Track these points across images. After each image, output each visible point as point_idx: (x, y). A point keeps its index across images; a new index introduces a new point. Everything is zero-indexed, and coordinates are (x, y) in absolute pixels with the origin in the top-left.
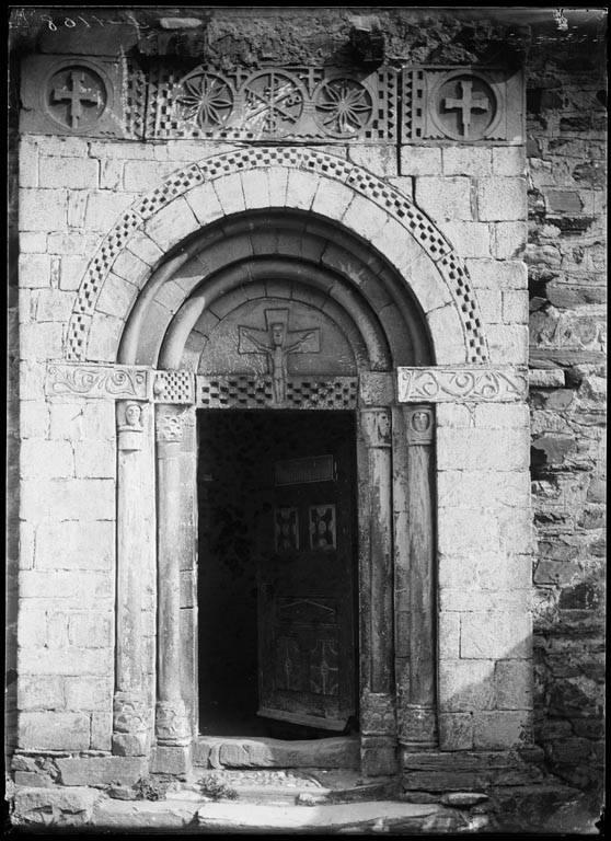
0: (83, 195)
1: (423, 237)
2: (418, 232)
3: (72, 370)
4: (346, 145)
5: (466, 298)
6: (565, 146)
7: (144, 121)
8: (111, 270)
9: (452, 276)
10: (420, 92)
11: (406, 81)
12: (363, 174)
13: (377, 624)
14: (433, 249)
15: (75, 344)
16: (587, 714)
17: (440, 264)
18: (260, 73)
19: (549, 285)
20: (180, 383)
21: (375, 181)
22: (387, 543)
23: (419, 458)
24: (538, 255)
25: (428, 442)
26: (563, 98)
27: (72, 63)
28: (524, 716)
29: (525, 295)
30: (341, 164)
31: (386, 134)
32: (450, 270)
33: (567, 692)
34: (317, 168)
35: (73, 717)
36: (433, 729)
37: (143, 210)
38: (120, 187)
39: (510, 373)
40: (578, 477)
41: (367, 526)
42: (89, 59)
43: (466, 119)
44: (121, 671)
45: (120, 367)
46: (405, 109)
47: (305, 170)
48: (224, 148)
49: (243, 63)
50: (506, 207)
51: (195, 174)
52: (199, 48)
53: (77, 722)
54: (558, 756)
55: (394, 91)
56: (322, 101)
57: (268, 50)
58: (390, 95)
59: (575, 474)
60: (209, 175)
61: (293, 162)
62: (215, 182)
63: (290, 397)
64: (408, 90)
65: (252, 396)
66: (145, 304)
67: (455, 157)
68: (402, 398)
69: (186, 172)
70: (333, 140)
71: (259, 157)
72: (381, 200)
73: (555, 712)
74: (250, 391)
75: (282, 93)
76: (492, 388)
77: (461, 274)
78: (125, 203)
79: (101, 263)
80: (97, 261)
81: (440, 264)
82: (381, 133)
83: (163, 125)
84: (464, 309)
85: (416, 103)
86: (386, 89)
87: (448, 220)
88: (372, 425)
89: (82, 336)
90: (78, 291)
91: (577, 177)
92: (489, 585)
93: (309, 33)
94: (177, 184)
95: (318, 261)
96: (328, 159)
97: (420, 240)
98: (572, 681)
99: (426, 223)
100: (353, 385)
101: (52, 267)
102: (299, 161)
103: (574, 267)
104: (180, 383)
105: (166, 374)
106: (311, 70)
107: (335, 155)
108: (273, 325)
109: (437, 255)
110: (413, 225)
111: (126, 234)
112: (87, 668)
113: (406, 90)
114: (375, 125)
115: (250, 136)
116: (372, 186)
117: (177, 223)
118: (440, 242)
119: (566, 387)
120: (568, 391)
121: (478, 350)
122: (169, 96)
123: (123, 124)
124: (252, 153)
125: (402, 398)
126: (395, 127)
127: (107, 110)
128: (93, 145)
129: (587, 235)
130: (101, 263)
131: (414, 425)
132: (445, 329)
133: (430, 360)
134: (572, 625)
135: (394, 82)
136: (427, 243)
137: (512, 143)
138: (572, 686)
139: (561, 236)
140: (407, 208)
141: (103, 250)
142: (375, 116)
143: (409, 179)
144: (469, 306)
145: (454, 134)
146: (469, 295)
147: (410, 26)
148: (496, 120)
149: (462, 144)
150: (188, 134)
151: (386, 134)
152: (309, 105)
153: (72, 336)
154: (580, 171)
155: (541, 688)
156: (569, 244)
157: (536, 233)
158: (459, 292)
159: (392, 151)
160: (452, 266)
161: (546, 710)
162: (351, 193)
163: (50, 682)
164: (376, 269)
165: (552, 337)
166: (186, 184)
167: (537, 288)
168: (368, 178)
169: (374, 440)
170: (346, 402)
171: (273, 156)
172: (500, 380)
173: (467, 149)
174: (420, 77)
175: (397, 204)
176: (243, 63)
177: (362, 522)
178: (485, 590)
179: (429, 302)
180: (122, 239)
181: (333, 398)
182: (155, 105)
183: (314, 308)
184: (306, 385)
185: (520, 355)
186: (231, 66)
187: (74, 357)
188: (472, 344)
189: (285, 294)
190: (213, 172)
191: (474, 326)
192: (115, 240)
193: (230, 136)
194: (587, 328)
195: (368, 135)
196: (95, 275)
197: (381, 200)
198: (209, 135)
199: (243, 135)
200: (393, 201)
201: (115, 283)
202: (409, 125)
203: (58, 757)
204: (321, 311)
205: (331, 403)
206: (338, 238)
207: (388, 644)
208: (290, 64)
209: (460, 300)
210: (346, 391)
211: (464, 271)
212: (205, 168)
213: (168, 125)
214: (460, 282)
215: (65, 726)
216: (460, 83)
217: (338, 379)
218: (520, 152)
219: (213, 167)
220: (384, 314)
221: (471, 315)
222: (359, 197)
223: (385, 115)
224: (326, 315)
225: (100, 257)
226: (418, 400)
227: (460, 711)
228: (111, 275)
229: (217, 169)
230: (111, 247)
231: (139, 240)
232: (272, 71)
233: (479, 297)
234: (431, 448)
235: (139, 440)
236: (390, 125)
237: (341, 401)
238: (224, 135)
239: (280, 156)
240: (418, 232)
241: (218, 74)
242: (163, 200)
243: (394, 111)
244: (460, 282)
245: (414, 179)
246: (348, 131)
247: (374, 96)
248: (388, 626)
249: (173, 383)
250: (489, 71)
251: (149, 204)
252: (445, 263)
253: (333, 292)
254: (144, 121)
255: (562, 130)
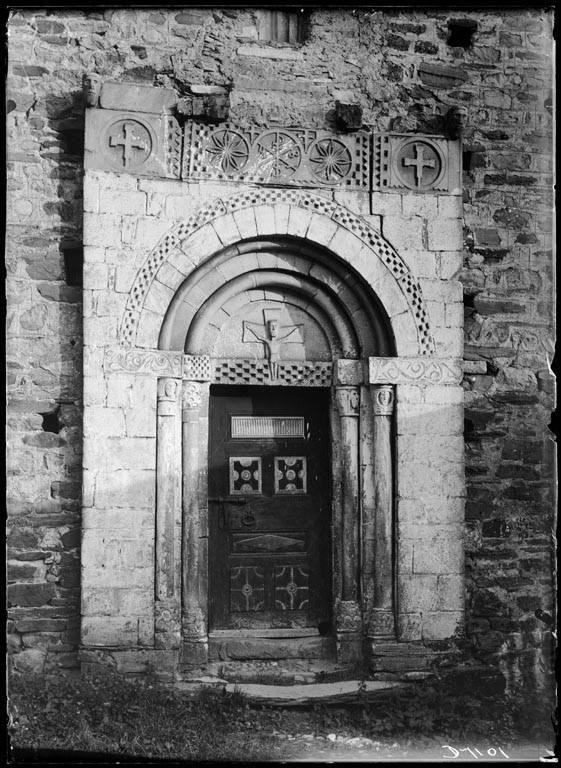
0: (134, 219)
1: (388, 261)
2: (384, 257)
3: (124, 353)
4: (332, 190)
5: (419, 307)
6: (488, 196)
7: (181, 164)
8: (155, 278)
9: (409, 290)
10: (386, 153)
11: (376, 143)
12: (344, 212)
13: (348, 549)
14: (395, 270)
15: (127, 334)
16: (501, 614)
17: (400, 282)
18: (268, 132)
19: (476, 299)
20: (202, 365)
21: (353, 217)
22: (356, 488)
23: (384, 425)
24: (468, 275)
25: (390, 413)
26: (487, 159)
27: (125, 117)
28: (458, 616)
29: (461, 306)
30: (329, 204)
31: (361, 183)
32: (408, 286)
33: (487, 598)
34: (311, 206)
35: (124, 621)
36: (393, 626)
37: (180, 232)
38: (163, 214)
39: (450, 363)
40: (496, 441)
41: (340, 476)
42: (139, 114)
43: (420, 174)
44: (160, 585)
45: (160, 352)
46: (376, 165)
47: (302, 207)
48: (243, 188)
49: (256, 124)
50: (448, 240)
51: (220, 206)
52: (225, 111)
53: (128, 623)
54: (480, 645)
55: (367, 151)
56: (315, 155)
57: (275, 115)
58: (364, 154)
59: (494, 438)
60: (230, 208)
61: (294, 200)
62: (235, 214)
63: (283, 376)
64: (378, 151)
65: (253, 375)
66: (178, 303)
67: (411, 201)
68: (373, 380)
69: (213, 205)
70: (322, 186)
71: (268, 196)
72: (358, 233)
73: (478, 613)
74: (252, 371)
75: (285, 147)
76: (438, 373)
77: (415, 289)
78: (166, 227)
79: (148, 272)
80: (144, 271)
81: (400, 282)
82: (358, 182)
83: (195, 169)
84: (418, 315)
85: (384, 161)
86: (361, 148)
87: (406, 249)
88: (346, 399)
89: (133, 328)
90: (129, 293)
91: (496, 219)
92: (434, 519)
93: (305, 104)
94: (206, 213)
95: (306, 274)
96: (318, 200)
97: (386, 263)
98: (490, 589)
99: (390, 250)
100: (328, 368)
101: (109, 274)
102: (298, 200)
103: (494, 286)
104: (202, 365)
105: (191, 358)
106: (307, 132)
107: (324, 197)
108: (269, 322)
109: (398, 275)
110: (381, 251)
111: (167, 250)
112: (135, 583)
113: (376, 150)
114: (354, 176)
115: (262, 179)
116: (351, 221)
117: (204, 244)
118: (401, 265)
119: (487, 374)
120: (489, 377)
121: (427, 346)
122: (200, 146)
123: (165, 166)
124: (263, 192)
125: (373, 380)
126: (368, 178)
127: (152, 154)
128: (141, 181)
129: (504, 262)
130: (148, 272)
131: (380, 400)
132: (403, 329)
133: (392, 352)
134: (491, 549)
135: (367, 143)
136: (391, 266)
137: (453, 193)
138: (492, 594)
139: (484, 262)
140: (378, 240)
141: (149, 262)
142: (353, 169)
143: (378, 218)
144: (421, 314)
145: (413, 187)
146: (422, 305)
147: (377, 101)
148: (442, 173)
149: (417, 193)
150: (215, 176)
151: (361, 183)
152: (305, 158)
153: (124, 327)
154: (499, 215)
155: (468, 595)
156: (489, 269)
157: (467, 260)
158: (414, 303)
159: (366, 195)
160: (409, 283)
161: (472, 611)
162: (335, 226)
163: (107, 593)
164: (352, 283)
165: (478, 337)
166: (213, 214)
167: (468, 300)
168: (348, 215)
169: (347, 410)
170: (323, 381)
171: (279, 195)
172: (444, 368)
173: (420, 197)
174: (387, 141)
175: (370, 235)
176: (256, 124)
177: (335, 472)
178: (431, 523)
179: (393, 310)
180: (164, 254)
181: (314, 377)
182: (189, 152)
183: (301, 309)
184: (295, 368)
185: (457, 350)
186: (248, 125)
187: (126, 343)
188: (423, 341)
189: (279, 297)
190: (233, 206)
191: (424, 328)
192: (159, 255)
193: (246, 179)
194: (503, 331)
195: (349, 183)
196: (143, 282)
197: (358, 233)
198: (231, 177)
199: (256, 179)
200: (366, 233)
201: (158, 288)
202: (378, 177)
203: (113, 651)
204: (305, 311)
205: (312, 381)
206: (323, 258)
207: (356, 564)
208: (292, 127)
209: (415, 309)
210: (323, 372)
211: (417, 287)
212: (227, 203)
213: (199, 169)
214: (415, 296)
215: (118, 627)
216: (415, 147)
217: (318, 364)
218: (457, 200)
219: (233, 202)
220: (355, 315)
221: (423, 320)
222: (341, 229)
223: (361, 168)
224: (309, 314)
225: (146, 267)
226: (384, 382)
227: (413, 612)
228: (155, 282)
229: (236, 204)
230: (155, 260)
231: (177, 256)
232: (278, 131)
233: (429, 307)
234: (393, 418)
235: (172, 408)
236: (365, 176)
237: (320, 380)
238: (242, 178)
239: (284, 195)
240: (384, 257)
241: (237, 131)
242: (195, 225)
243: (367, 165)
244: (415, 296)
245: (382, 217)
246: (334, 179)
247: (353, 154)
248: (356, 550)
249: (197, 365)
250: (437, 139)
251: (184, 229)
252: (404, 280)
253: (316, 297)
254: (181, 164)
255: (486, 183)
